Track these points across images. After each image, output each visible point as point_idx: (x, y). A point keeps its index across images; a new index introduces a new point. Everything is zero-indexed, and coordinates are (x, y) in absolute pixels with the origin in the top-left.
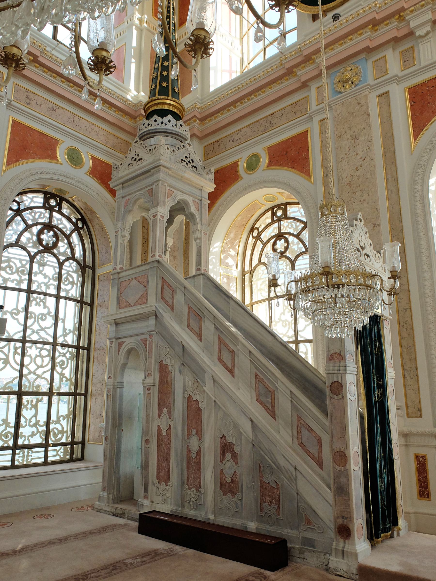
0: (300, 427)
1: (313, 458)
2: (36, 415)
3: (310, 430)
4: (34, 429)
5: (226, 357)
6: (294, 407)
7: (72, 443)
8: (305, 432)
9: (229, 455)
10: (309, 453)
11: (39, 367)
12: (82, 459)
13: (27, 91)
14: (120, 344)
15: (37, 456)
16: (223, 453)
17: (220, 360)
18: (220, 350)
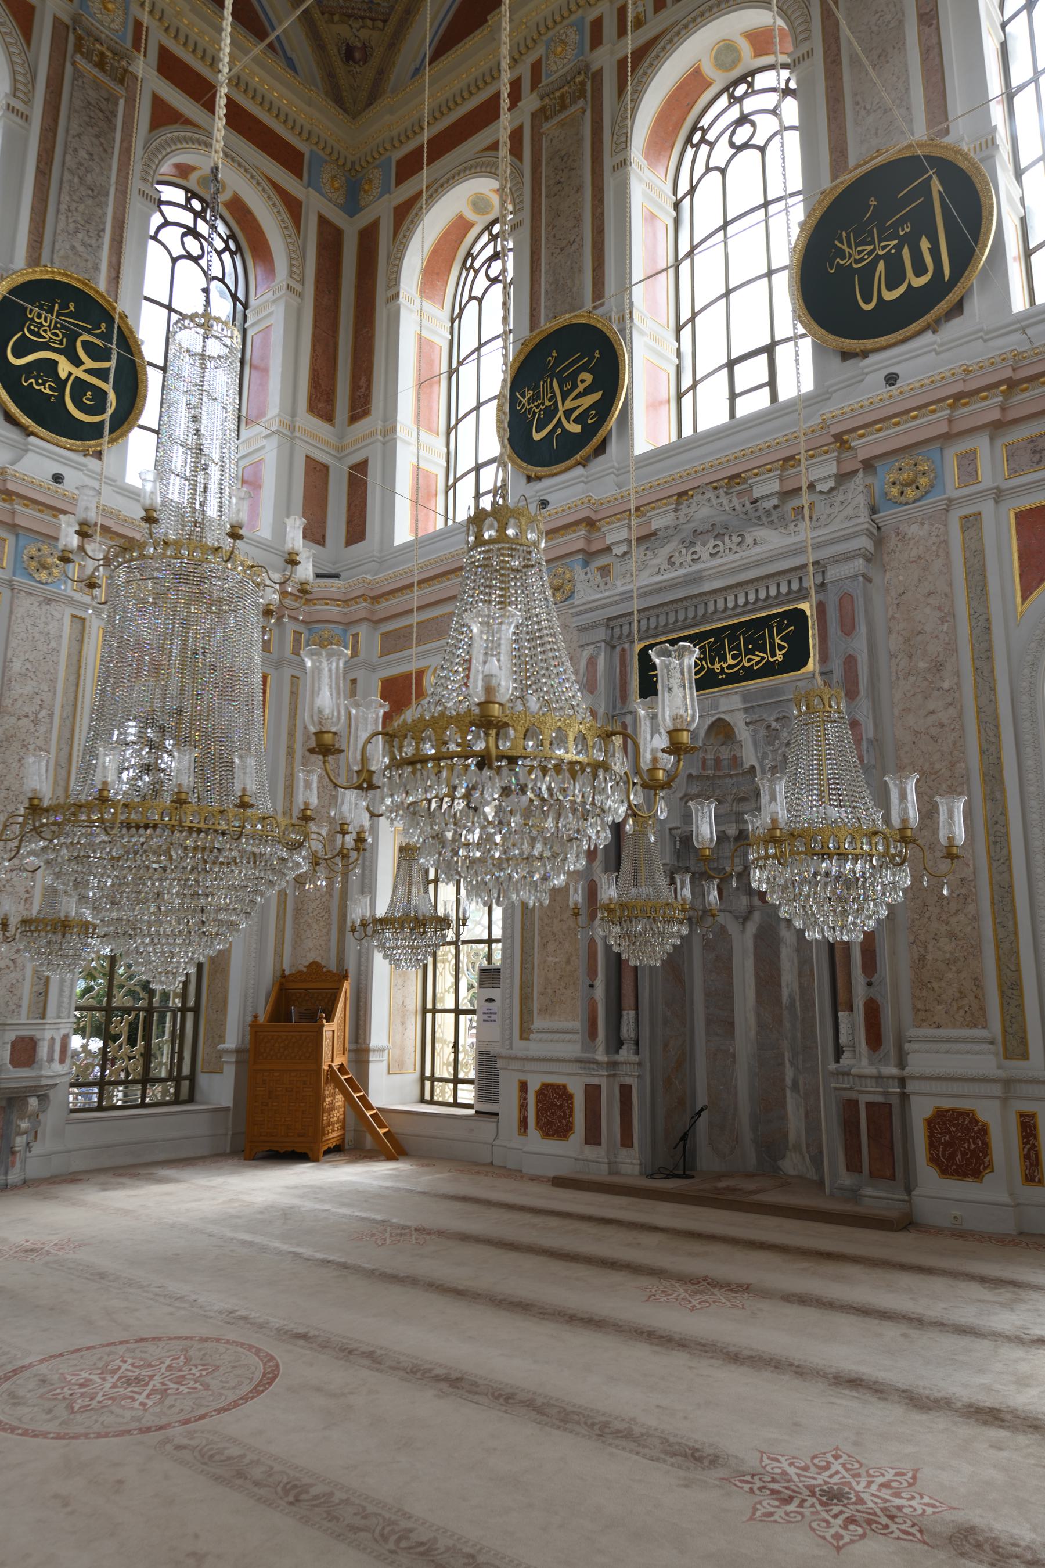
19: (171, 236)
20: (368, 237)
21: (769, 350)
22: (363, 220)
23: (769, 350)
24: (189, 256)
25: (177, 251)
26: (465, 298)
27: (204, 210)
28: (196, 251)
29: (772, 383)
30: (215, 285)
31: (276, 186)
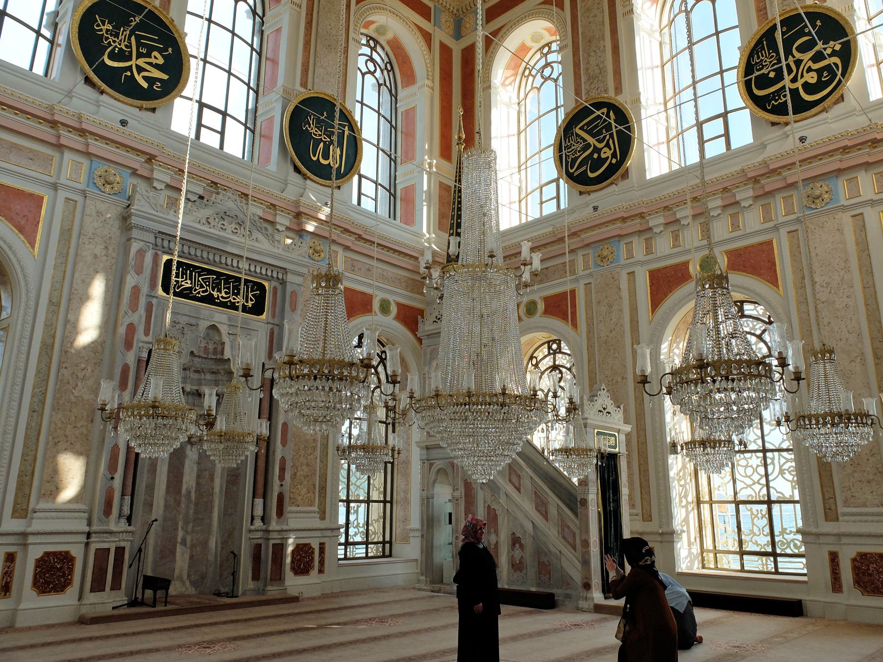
0: (563, 526)
1: (571, 545)
2: (357, 519)
3: (569, 527)
4: (356, 530)
5: (515, 479)
6: (559, 514)
7: (384, 543)
8: (566, 530)
9: (517, 545)
10: (568, 542)
11: (358, 479)
12: (390, 556)
13: (353, 260)
14: (431, 465)
15: (360, 551)
16: (514, 545)
17: (510, 481)
18: (510, 474)
19: (361, 62)
20: (468, 54)
21: (724, 115)
22: (465, 43)
23: (724, 115)
24: (369, 72)
25: (364, 70)
26: (529, 88)
27: (375, 46)
28: (372, 69)
29: (727, 135)
30: (383, 88)
31: (420, 29)
